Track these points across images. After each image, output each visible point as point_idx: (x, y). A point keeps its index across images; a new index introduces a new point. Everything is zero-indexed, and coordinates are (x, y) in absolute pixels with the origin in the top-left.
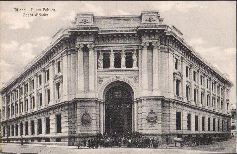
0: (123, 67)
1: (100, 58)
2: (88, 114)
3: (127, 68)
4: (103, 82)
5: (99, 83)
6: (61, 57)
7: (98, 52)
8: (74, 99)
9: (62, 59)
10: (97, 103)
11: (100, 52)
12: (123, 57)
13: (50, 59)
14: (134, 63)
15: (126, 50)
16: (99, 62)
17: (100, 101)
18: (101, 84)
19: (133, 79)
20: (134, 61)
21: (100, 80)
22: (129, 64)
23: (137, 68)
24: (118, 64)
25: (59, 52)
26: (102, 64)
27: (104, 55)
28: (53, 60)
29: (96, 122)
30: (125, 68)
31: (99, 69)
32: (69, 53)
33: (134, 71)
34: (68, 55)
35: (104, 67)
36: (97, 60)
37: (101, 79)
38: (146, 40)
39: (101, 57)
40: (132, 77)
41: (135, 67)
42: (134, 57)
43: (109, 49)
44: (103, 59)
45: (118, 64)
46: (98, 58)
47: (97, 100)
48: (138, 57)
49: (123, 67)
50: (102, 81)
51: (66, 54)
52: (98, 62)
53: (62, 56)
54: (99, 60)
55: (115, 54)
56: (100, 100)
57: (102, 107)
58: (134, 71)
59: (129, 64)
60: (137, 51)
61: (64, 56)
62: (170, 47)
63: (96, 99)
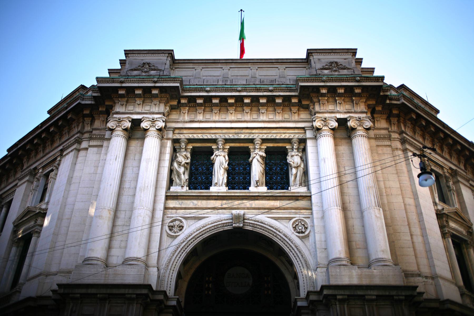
0: (258, 188)
1: (181, 158)
4: (182, 235)
5: (169, 235)
7: (176, 141)
12: (258, 157)
15: (264, 141)
17: (161, 302)
18: (177, 236)
20: (294, 171)
23: (303, 190)
25: (56, 145)
26: (184, 177)
30: (263, 189)
31: (173, 189)
33: (296, 198)
35: (192, 184)
37: (177, 223)
38: (330, 113)
39: (184, 157)
40: (290, 219)
41: (296, 189)
42: (294, 159)
43: (213, 137)
46: (173, 159)
47: (146, 296)
48: (304, 159)
49: (258, 188)
50: (181, 228)
52: (171, 171)
54: (175, 165)
55: (232, 153)
61: (67, 154)
63: (145, 291)
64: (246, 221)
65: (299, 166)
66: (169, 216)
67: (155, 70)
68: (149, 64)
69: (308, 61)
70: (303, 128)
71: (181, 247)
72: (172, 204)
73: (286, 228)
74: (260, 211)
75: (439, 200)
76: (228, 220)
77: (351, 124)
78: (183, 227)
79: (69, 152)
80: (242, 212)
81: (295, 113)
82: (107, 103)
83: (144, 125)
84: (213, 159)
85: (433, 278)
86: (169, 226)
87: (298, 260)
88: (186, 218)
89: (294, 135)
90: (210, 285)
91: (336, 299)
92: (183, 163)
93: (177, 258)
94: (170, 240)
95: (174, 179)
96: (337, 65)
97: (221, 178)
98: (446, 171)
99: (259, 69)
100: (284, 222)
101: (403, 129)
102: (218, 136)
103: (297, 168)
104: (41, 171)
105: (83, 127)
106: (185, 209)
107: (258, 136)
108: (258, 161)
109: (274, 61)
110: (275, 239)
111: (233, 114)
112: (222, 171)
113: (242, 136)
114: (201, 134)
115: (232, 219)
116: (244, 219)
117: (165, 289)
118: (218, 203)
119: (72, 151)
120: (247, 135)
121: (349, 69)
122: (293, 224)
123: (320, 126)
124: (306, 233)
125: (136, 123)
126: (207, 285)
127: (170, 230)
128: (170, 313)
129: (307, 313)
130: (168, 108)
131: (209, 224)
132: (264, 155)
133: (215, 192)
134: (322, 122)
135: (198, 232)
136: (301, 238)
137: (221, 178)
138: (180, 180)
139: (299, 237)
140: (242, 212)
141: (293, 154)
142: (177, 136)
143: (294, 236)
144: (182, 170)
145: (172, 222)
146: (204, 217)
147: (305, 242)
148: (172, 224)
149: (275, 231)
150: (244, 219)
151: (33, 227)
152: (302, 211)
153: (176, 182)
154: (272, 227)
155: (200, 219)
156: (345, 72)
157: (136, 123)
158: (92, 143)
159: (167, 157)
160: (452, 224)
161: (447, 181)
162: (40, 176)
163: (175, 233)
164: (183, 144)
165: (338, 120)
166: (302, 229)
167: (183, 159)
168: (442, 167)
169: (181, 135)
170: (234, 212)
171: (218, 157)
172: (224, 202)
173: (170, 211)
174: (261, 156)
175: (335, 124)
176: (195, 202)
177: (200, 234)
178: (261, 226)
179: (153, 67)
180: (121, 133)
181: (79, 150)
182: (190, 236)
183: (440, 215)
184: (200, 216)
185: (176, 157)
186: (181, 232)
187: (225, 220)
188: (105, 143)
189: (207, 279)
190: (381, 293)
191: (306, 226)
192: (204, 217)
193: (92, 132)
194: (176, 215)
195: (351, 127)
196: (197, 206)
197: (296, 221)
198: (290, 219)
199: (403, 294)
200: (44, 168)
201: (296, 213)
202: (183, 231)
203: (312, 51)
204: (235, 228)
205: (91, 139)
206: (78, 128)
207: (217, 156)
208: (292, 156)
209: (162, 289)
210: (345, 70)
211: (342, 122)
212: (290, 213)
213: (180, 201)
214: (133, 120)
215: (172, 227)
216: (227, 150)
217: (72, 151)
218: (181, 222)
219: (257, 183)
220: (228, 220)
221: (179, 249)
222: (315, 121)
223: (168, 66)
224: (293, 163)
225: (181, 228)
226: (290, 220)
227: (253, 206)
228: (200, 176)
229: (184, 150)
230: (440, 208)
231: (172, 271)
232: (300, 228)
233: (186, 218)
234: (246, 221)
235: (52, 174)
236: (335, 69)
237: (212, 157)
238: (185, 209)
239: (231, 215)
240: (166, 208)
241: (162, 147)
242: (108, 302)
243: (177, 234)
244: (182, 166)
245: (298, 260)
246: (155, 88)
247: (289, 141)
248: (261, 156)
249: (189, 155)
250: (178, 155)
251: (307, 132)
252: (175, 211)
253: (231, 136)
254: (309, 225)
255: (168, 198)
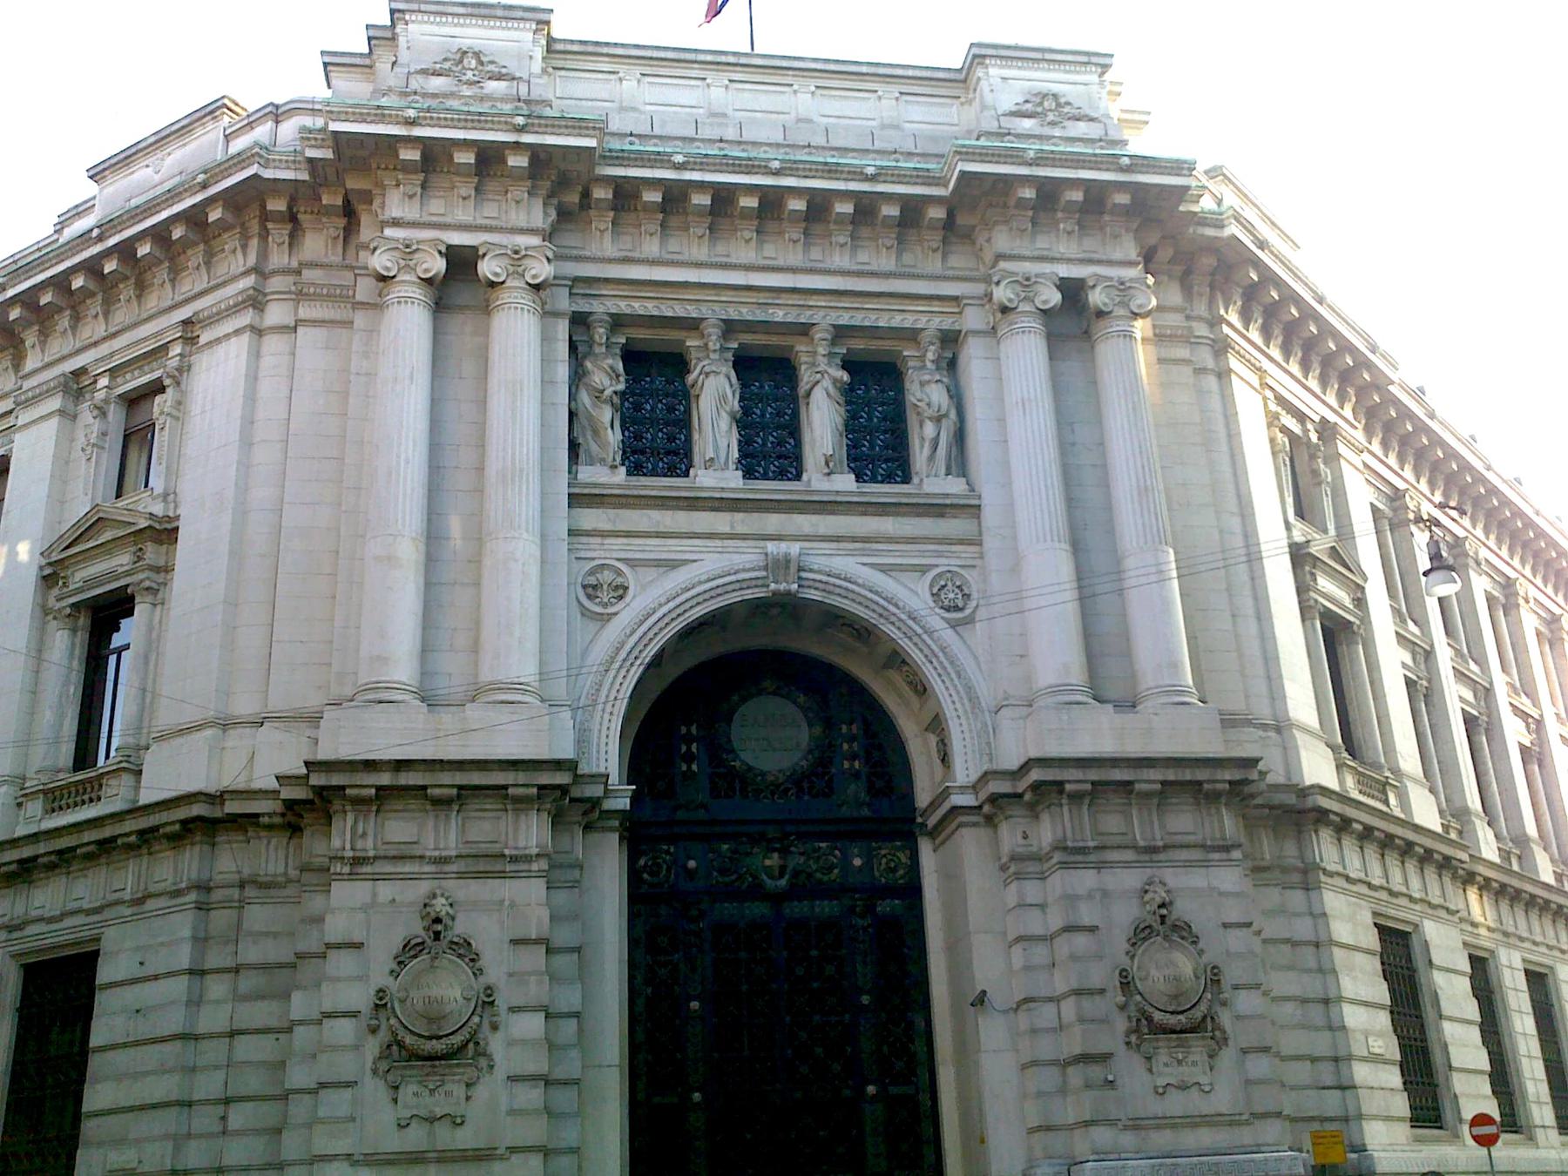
2: (465, 950)
3: (859, 478)
4: (628, 613)
6: (176, 349)
7: (580, 321)
8: (307, 764)
9: (184, 368)
10: (557, 820)
11: (600, 333)
12: (827, 383)
13: (30, 364)
14: (924, 439)
16: (590, 417)
17: (595, 803)
19: (923, 586)
20: (929, 429)
21: (599, 592)
22: (879, 446)
24: (770, 446)
25: (152, 302)
26: (614, 437)
27: (634, 358)
28: (78, 373)
29: (552, 1046)
31: (586, 473)
32: (276, 314)
33: (937, 509)
34: (258, 332)
35: (636, 458)
36: (572, 397)
37: (607, 577)
39: (607, 375)
40: (923, 569)
41: (932, 481)
42: (925, 392)
43: (693, 312)
44: (621, 387)
45: (770, 446)
46: (577, 376)
47: (563, 790)
48: (957, 396)
50: (621, 591)
51: (246, 318)
52: (572, 415)
53: (190, 340)
54: (585, 398)
55: (747, 365)
56: (596, 791)
57: (607, 870)
58: (937, 509)
59: (879, 446)
60: (951, 340)
61: (218, 341)
62: (1226, 329)
63: (562, 778)
64: (804, 575)
65: (946, 415)
66: (582, 554)
67: (499, 77)
68: (477, 55)
69: (965, 81)
70: (956, 299)
71: (628, 647)
72: (591, 518)
73: (913, 595)
74: (842, 545)
75: (1297, 514)
76: (753, 569)
77: (1096, 298)
78: (626, 588)
79: (227, 336)
80: (794, 548)
81: (934, 251)
82: (353, 183)
83: (487, 268)
84: (696, 381)
85: (1278, 730)
86: (584, 587)
87: (948, 683)
88: (632, 563)
89: (931, 322)
90: (694, 747)
91: (1061, 792)
92: (608, 392)
93: (619, 680)
94: (593, 626)
95: (581, 440)
96: (1059, 105)
97: (723, 443)
98: (1310, 426)
99: (820, 92)
100: (905, 577)
101: (1222, 312)
102: (705, 311)
103: (938, 420)
104: (103, 382)
105: (263, 254)
106: (629, 534)
107: (825, 318)
108: (826, 390)
109: (864, 69)
110: (887, 628)
111: (753, 243)
112: (725, 422)
113: (779, 315)
114: (655, 303)
115: (766, 568)
116: (800, 569)
117: (602, 770)
118: (721, 522)
119: (237, 332)
120: (795, 311)
121: (1092, 120)
122: (931, 586)
123: (1010, 300)
124: (967, 612)
125: (461, 263)
126: (684, 748)
127: (589, 597)
128: (611, 829)
129: (975, 825)
130: (553, 215)
131: (700, 583)
132: (846, 377)
133: (713, 489)
134: (1018, 288)
135: (671, 605)
136: (954, 625)
137: (723, 443)
138: (603, 445)
139: (947, 621)
140: (794, 548)
141: (927, 377)
142: (583, 306)
143: (936, 621)
144: (606, 414)
145: (592, 572)
146: (686, 562)
147: (965, 635)
148: (592, 580)
149: (882, 602)
150: (800, 569)
151: (128, 574)
152: (954, 548)
153: (588, 451)
154: (877, 593)
155: (673, 565)
156: (1080, 129)
157: (461, 263)
158: (305, 312)
159: (563, 372)
160: (1324, 583)
161: (1313, 457)
162: (106, 401)
163: (605, 605)
164: (602, 330)
165: (1065, 285)
166: (955, 602)
167: (607, 382)
168: (1301, 417)
169: (595, 303)
170: (771, 547)
171: (712, 377)
172: (739, 516)
173: (584, 539)
174: (835, 381)
175: (1055, 298)
176: (655, 515)
177: (679, 611)
178: (846, 589)
179: (491, 67)
180: (417, 292)
181: (258, 332)
182: (649, 615)
183: (1300, 557)
184: (673, 556)
185: (585, 373)
186: (621, 604)
187: (744, 570)
188: (360, 319)
189: (684, 730)
190: (1171, 775)
191: (966, 591)
192: (686, 562)
193: (299, 273)
194: (603, 554)
195: (1097, 307)
196: (662, 529)
197: (940, 575)
198: (923, 569)
199: (1228, 777)
200: (113, 372)
201: (939, 555)
202: (628, 599)
203: (983, 51)
204: (775, 593)
205: (300, 296)
206: (245, 255)
207: (707, 375)
208: (922, 384)
209: (594, 770)
210: (1081, 124)
211: (1072, 291)
212: (922, 554)
213: (611, 512)
214: (449, 247)
215: (594, 587)
216: (730, 355)
217: (237, 332)
218: (619, 573)
219: (827, 464)
220: (753, 569)
221: (623, 654)
222: (998, 283)
223: (537, 65)
224: (929, 405)
225: (621, 592)
226: (924, 572)
227: (822, 531)
228: (655, 435)
229: (603, 349)
230: (1298, 537)
231: (607, 716)
232: (951, 596)
233: (632, 563)
234: (804, 575)
235: (161, 404)
236: (1051, 117)
237: (691, 378)
238: (629, 534)
239: (763, 557)
240: (572, 533)
241: (546, 339)
242: (456, 807)
243: (611, 610)
244: (605, 402)
245: (948, 683)
246: (517, 145)
247: (912, 335)
248: (835, 381)
249: (620, 366)
250: (588, 364)
251: (969, 311)
252: (599, 540)
253: (746, 314)
254: (974, 588)
255: (575, 500)
